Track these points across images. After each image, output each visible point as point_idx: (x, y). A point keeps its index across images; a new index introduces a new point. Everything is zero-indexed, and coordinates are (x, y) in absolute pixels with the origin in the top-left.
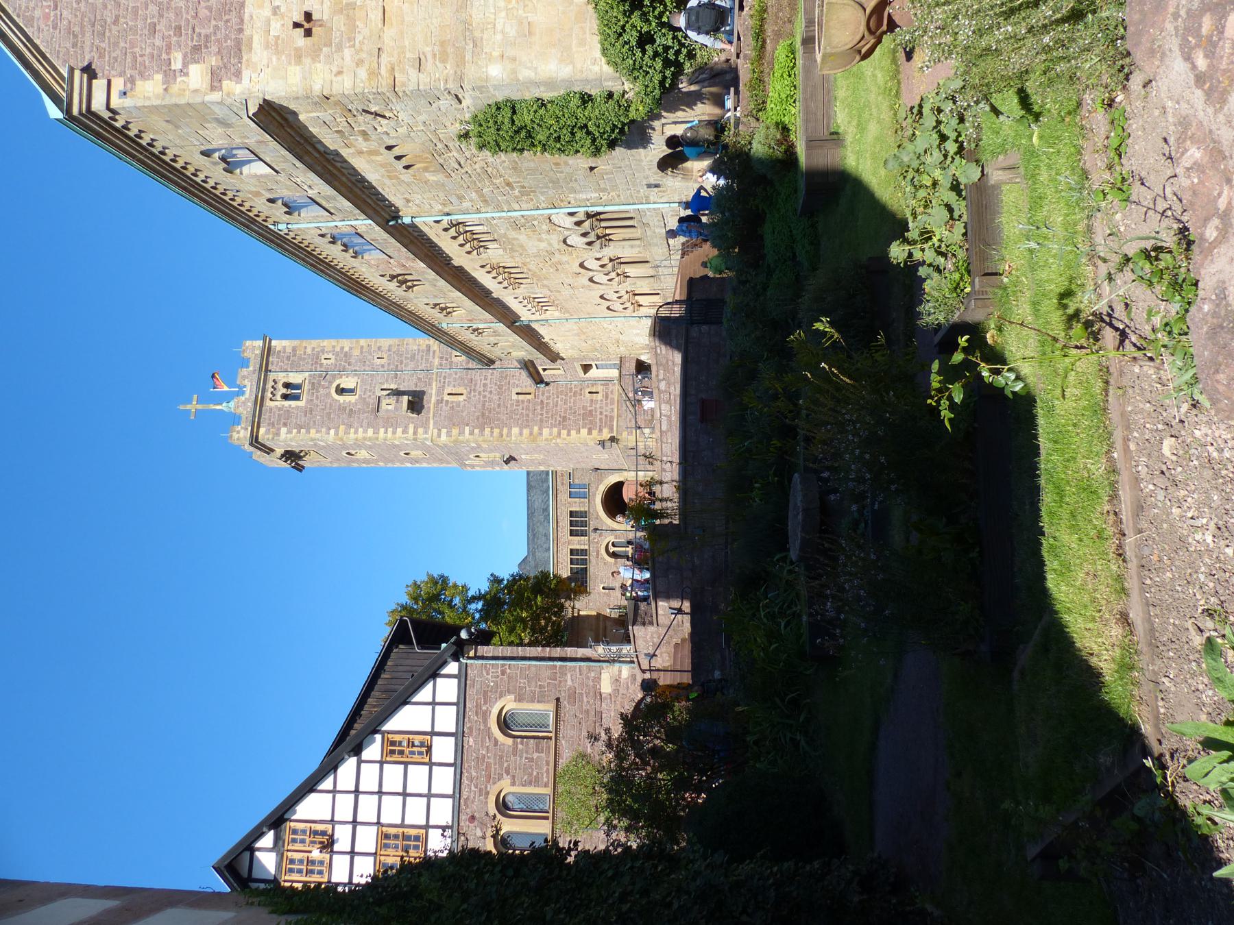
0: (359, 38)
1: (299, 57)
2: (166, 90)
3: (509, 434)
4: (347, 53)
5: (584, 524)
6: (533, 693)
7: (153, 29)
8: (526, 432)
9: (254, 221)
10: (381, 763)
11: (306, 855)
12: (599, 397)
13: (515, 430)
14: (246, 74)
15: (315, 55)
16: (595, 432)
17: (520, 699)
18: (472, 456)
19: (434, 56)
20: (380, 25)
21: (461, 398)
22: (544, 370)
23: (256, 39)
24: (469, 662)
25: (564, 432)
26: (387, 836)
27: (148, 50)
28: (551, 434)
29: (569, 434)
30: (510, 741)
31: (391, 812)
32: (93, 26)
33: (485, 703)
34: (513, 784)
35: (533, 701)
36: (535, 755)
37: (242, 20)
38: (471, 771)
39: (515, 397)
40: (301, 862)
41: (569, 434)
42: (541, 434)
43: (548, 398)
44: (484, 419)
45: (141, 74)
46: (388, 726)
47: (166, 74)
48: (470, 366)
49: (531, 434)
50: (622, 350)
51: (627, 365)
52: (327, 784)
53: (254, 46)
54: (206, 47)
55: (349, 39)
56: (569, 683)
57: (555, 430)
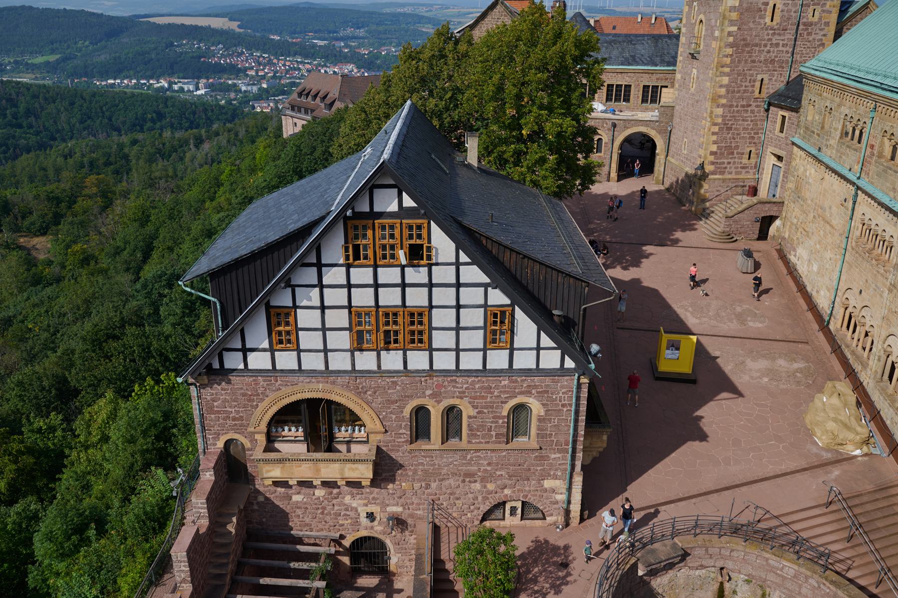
3: (723, 74)
5: (618, 99)
6: (546, 429)
8: (723, 91)
10: (485, 306)
11: (399, 241)
12: (745, 161)
13: (725, 80)
16: (712, 158)
17: (540, 420)
18: (702, 17)
21: (768, 20)
22: (784, 117)
24: (576, 381)
25: (716, 129)
26: (420, 314)
28: (717, 116)
29: (713, 134)
30: (505, 413)
31: (443, 318)
33: (538, 393)
34: (470, 417)
35: (538, 429)
36: (493, 433)
38: (479, 383)
39: (759, 78)
40: (392, 236)
41: (713, 134)
42: (718, 106)
43: (752, 112)
44: (742, 46)
46: (519, 314)
48: (801, 27)
49: (720, 97)
50: (792, 212)
51: (776, 209)
52: (464, 258)
56: (553, 456)
57: (720, 120)
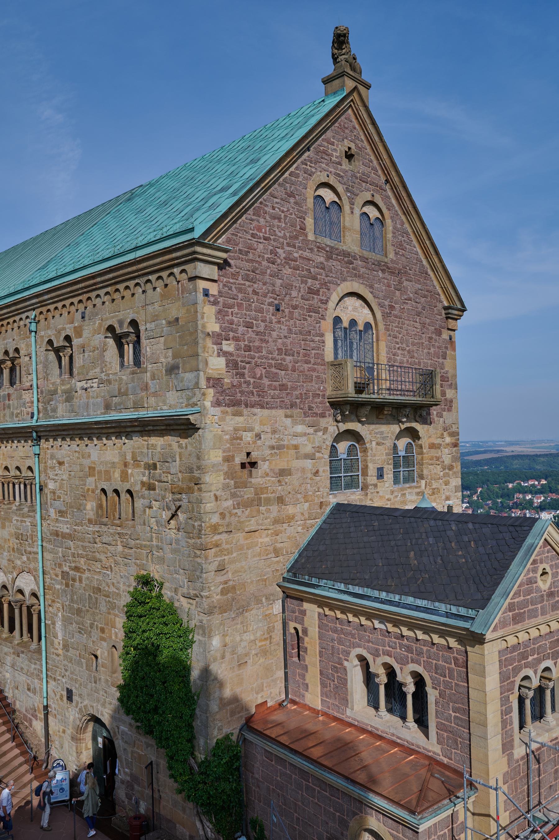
0: (239, 512)
1: (228, 459)
2: (209, 334)
4: (230, 503)
7: (249, 326)
9: (43, 304)
14: (217, 411)
15: (229, 475)
19: (226, 582)
20: (247, 529)
23: (241, 419)
27: (236, 320)
32: (253, 272)
37: (253, 406)
45: (219, 312)
47: (219, 335)
53: (237, 418)
54: (237, 374)
55: (238, 504)
